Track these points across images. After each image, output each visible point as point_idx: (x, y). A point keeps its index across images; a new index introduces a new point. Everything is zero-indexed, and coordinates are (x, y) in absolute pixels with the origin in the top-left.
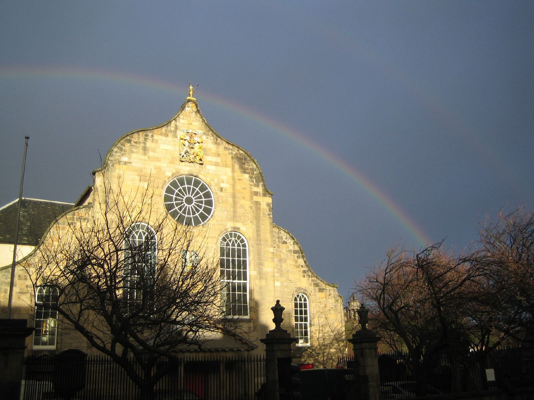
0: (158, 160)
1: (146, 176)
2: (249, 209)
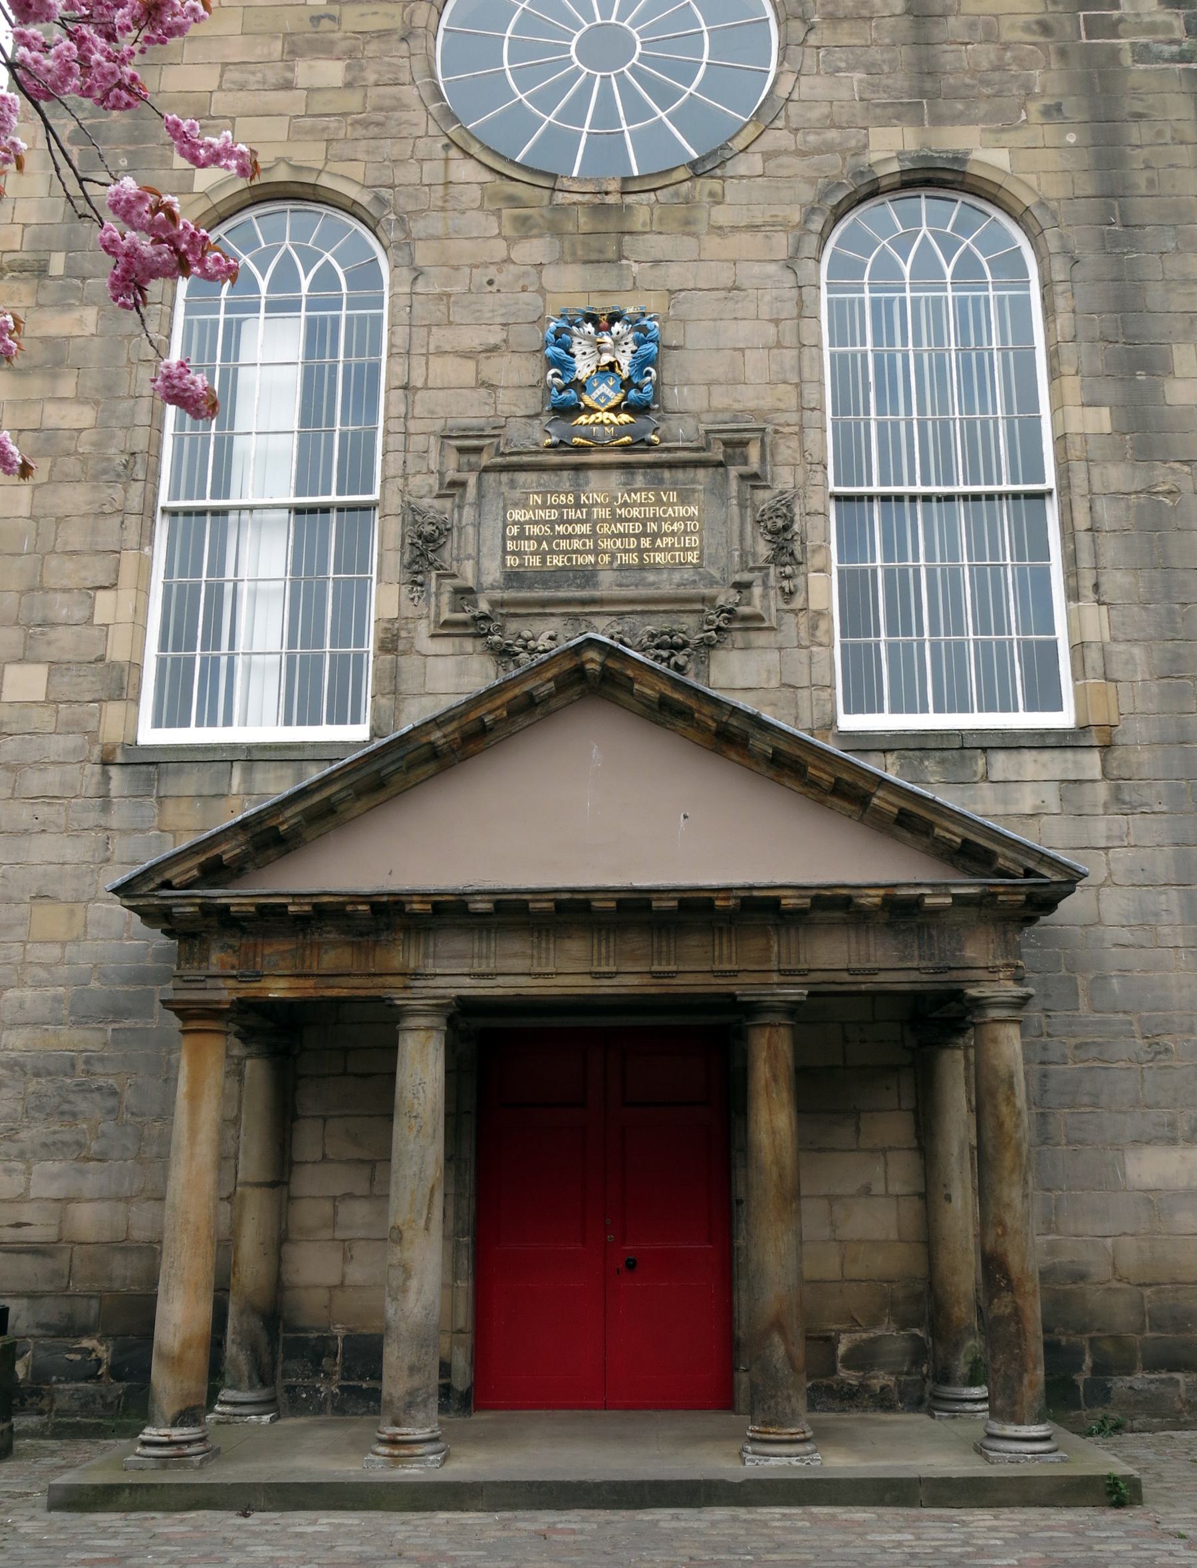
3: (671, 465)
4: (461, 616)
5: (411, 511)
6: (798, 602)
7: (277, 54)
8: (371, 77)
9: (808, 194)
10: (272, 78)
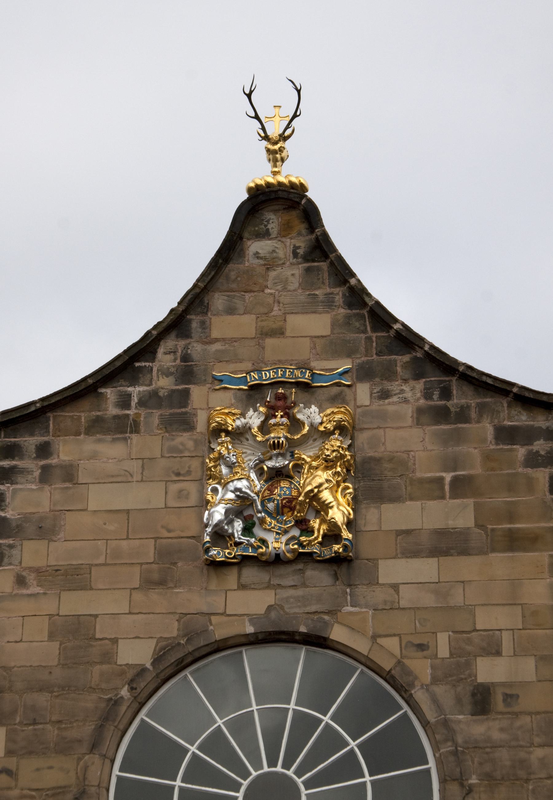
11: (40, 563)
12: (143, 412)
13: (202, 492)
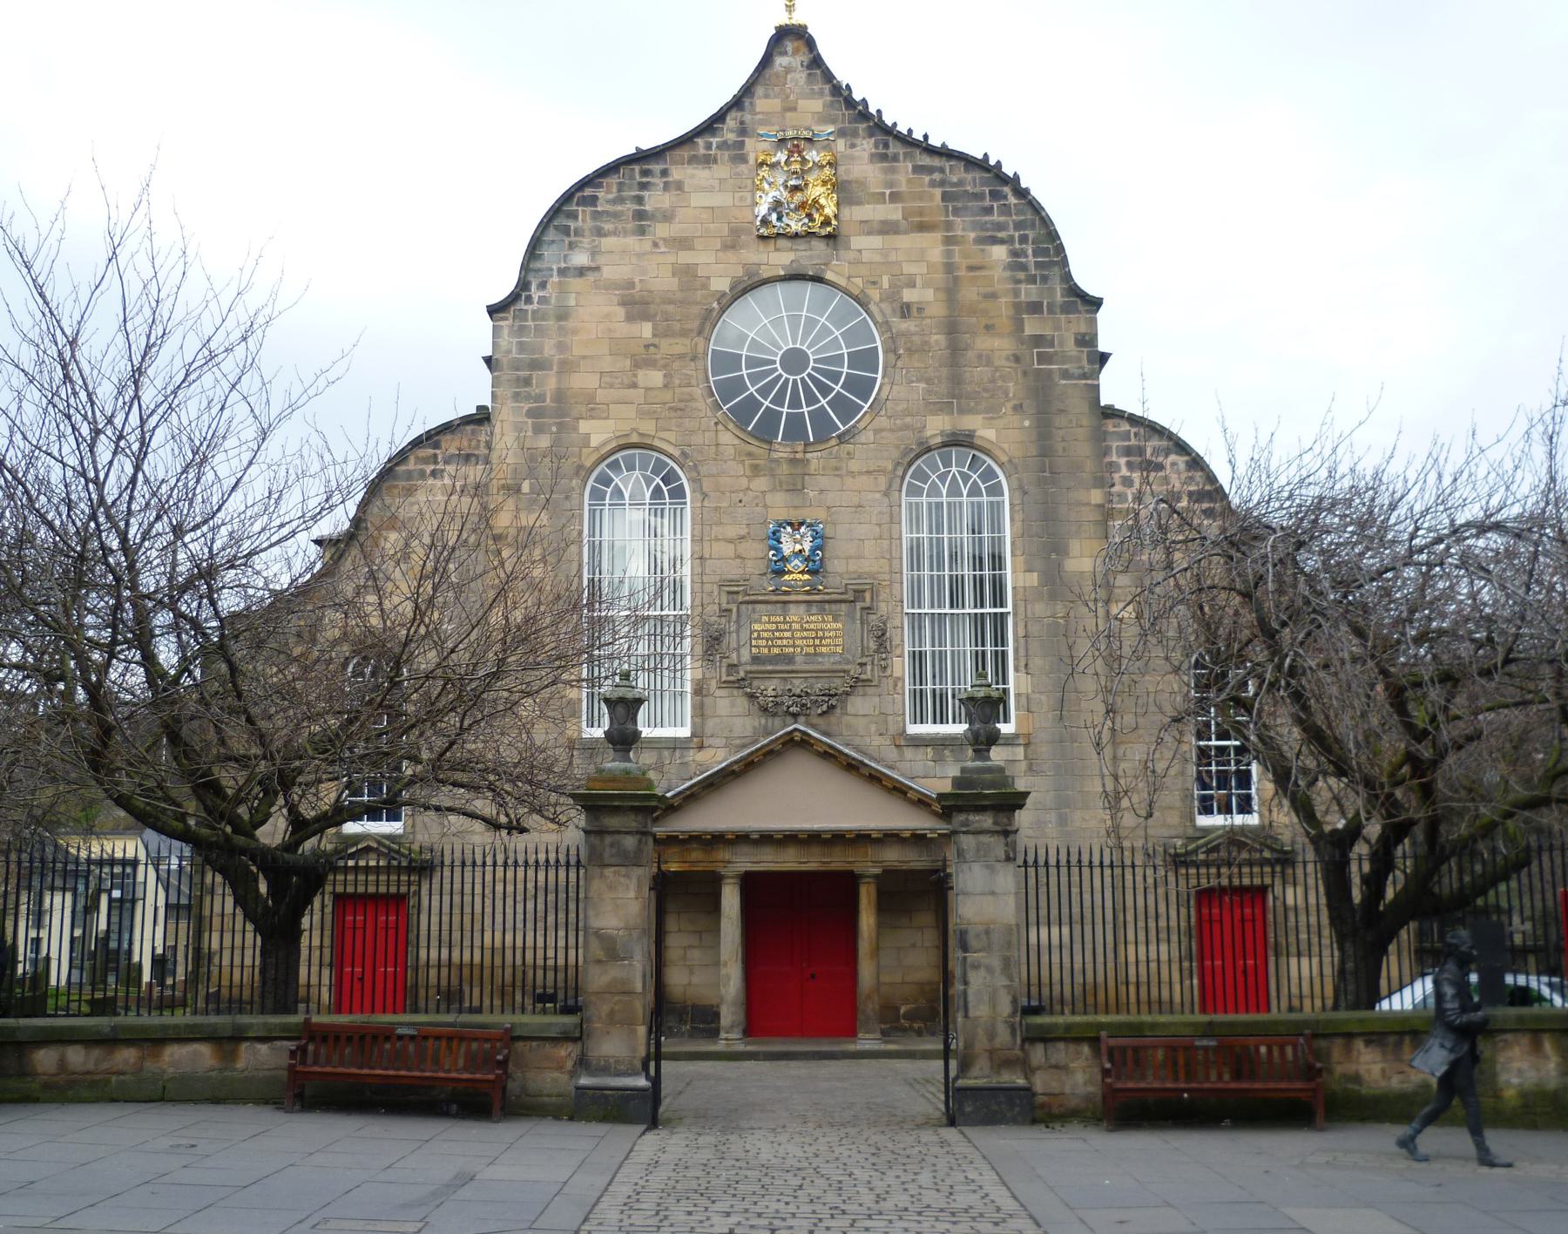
0: (684, 243)
1: (648, 303)
2: (1007, 364)
3: (829, 602)
4: (731, 678)
5: (705, 625)
6: (888, 672)
7: (628, 368)
8: (677, 382)
9: (896, 454)
10: (626, 382)
11: (666, 235)
12: (719, 153)
13: (753, 196)
